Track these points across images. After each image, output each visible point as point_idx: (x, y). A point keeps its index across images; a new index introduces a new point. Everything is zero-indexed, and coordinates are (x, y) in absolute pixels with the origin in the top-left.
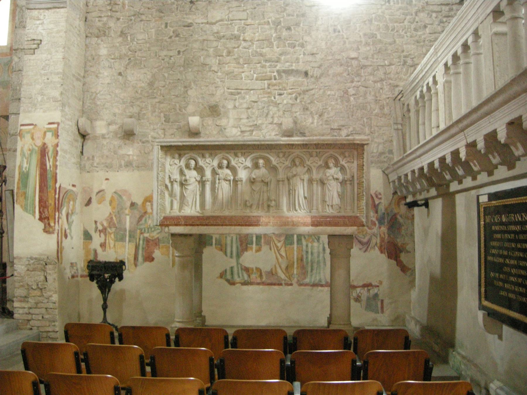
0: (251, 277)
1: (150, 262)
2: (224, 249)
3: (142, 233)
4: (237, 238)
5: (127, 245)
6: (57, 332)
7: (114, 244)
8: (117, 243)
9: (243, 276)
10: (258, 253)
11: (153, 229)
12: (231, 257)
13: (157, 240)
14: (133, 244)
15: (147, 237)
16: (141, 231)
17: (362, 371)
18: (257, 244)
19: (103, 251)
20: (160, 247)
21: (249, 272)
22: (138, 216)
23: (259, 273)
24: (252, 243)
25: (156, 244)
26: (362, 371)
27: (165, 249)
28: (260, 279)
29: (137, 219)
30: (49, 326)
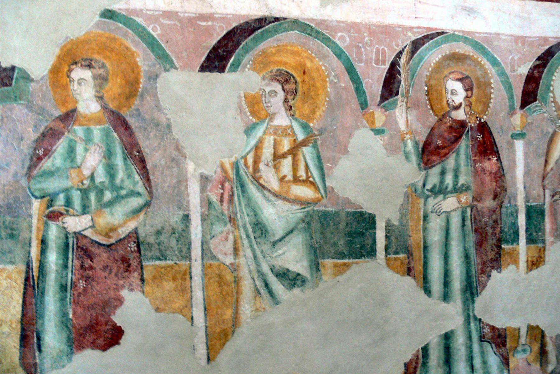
0: (512, 365)
2: (418, 267)
3: (54, 216)
4: (463, 220)
9: (484, 362)
10: (535, 272)
11: (108, 196)
12: (446, 297)
13: (133, 246)
14: (10, 267)
15: (78, 235)
16: (51, 203)
18: (530, 240)
20: (147, 275)
21: (504, 345)
22: (32, 135)
23: (536, 347)
24: (515, 239)
25: (125, 260)
27: (169, 285)
28: (538, 366)
29: (26, 148)
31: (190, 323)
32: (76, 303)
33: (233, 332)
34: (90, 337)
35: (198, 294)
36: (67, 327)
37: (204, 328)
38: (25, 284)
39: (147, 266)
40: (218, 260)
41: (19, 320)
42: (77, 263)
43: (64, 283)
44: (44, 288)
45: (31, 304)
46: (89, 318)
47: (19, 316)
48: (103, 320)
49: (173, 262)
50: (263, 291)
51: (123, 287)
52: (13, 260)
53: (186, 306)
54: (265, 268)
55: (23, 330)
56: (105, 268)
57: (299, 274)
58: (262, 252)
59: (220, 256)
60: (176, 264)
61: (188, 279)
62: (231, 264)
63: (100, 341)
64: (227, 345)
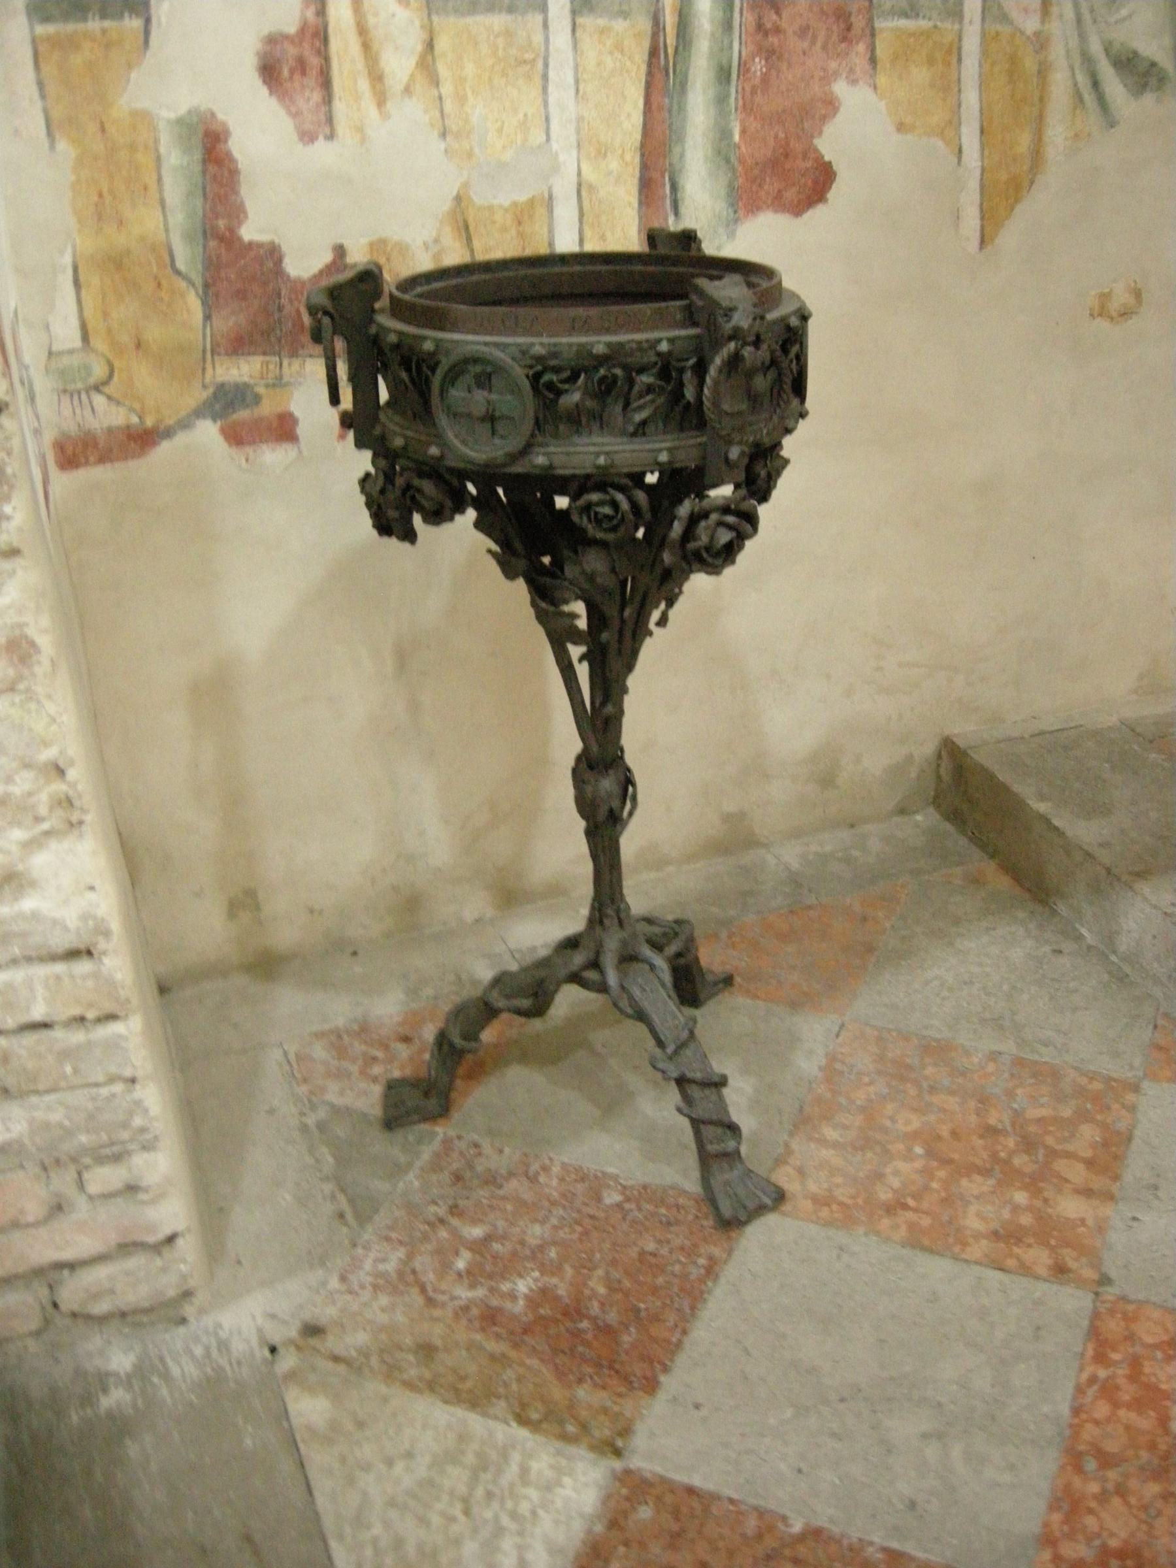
1: (798, 209)
5: (561, 39)
6: (171, 1239)
7: (414, 41)
8: (449, 29)
14: (619, 25)
17: (504, 499)
19: (307, 137)
26: (504, 499)
27: (920, 74)
30: (58, 1208)
31: (956, 160)
32: (747, 108)
33: (1032, 182)
34: (771, 185)
35: (971, 98)
36: (728, 161)
37: (978, 173)
38: (650, 65)
39: (882, 30)
40: (1011, 23)
41: (638, 144)
42: (750, 18)
43: (724, 62)
44: (686, 76)
45: (660, 108)
46: (771, 143)
47: (638, 136)
48: (797, 147)
49: (930, 24)
50: (1089, 97)
51: (836, 74)
52: (625, 8)
53: (950, 122)
54: (1096, 47)
55: (645, 167)
56: (804, 31)
57: (1153, 64)
58: (1092, 11)
59: (1015, 15)
60: (935, 27)
61: (954, 61)
62: (1037, 34)
63: (790, 194)
64: (1019, 208)
